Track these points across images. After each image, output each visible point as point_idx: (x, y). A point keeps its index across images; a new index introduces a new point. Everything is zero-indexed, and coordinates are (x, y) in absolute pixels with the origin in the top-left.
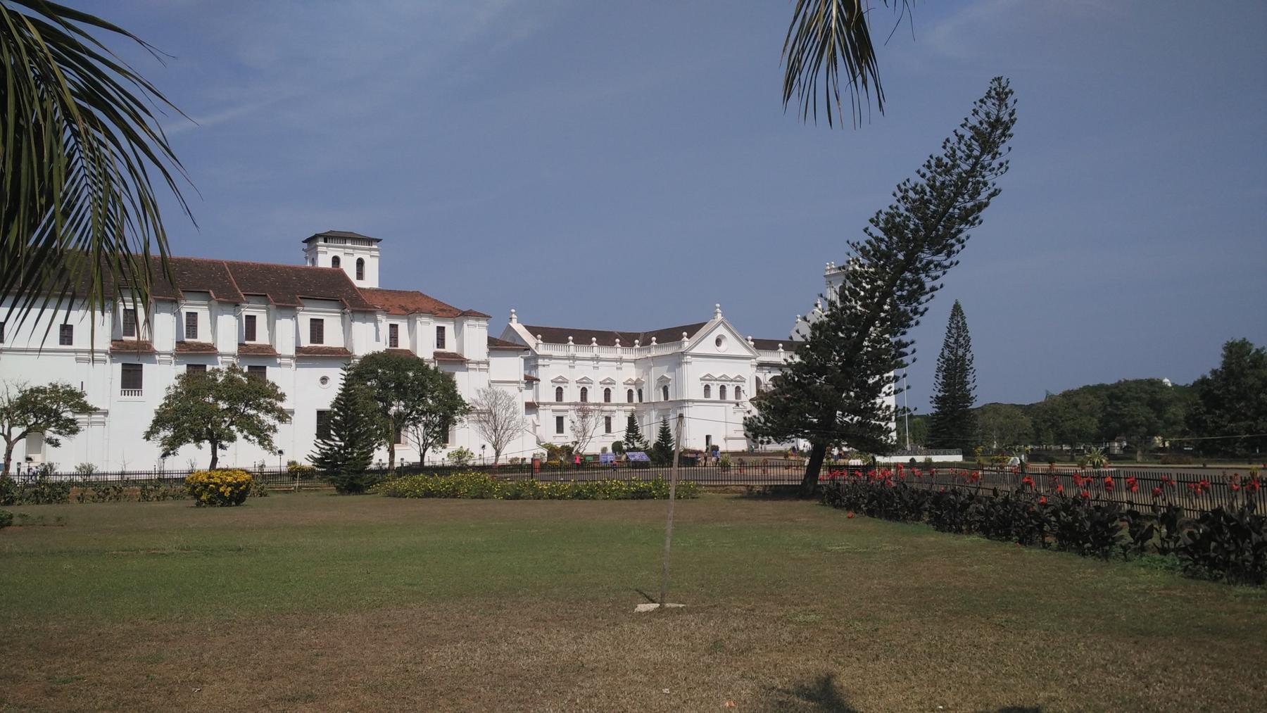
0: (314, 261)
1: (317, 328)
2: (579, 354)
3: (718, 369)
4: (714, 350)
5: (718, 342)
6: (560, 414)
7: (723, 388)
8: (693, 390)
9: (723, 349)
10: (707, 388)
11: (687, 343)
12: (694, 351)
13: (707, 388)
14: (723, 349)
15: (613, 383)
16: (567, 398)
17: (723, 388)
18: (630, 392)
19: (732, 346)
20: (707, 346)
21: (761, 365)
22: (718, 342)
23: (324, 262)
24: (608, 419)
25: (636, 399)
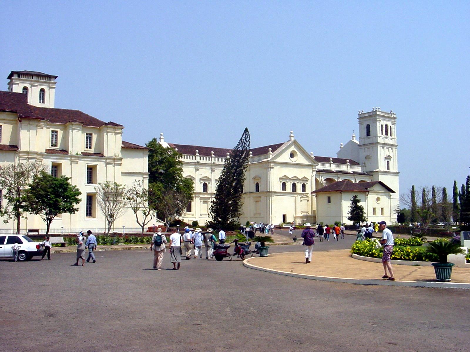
0: (10, 88)
2: (201, 161)
3: (291, 172)
5: (292, 155)
7: (294, 185)
8: (276, 186)
9: (294, 160)
10: (284, 185)
11: (271, 155)
12: (278, 160)
13: (284, 185)
14: (294, 160)
15: (209, 180)
16: (209, 191)
17: (294, 185)
19: (300, 159)
20: (285, 158)
21: (319, 171)
22: (292, 155)
23: (18, 89)
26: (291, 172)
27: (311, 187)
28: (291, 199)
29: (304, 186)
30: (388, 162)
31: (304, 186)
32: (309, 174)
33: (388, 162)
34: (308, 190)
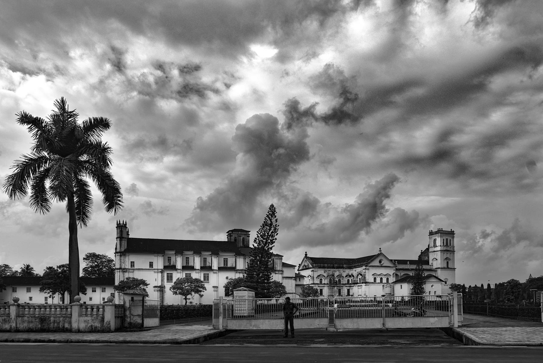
1: (226, 261)
4: (379, 264)
5: (380, 262)
6: (321, 288)
7: (381, 279)
10: (375, 279)
13: (375, 279)
17: (381, 279)
18: (348, 280)
20: (376, 263)
22: (380, 262)
24: (340, 290)
25: (350, 282)
26: (379, 271)
27: (392, 279)
28: (381, 286)
29: (388, 279)
30: (448, 262)
31: (388, 279)
32: (391, 272)
33: (448, 262)
34: (390, 281)
